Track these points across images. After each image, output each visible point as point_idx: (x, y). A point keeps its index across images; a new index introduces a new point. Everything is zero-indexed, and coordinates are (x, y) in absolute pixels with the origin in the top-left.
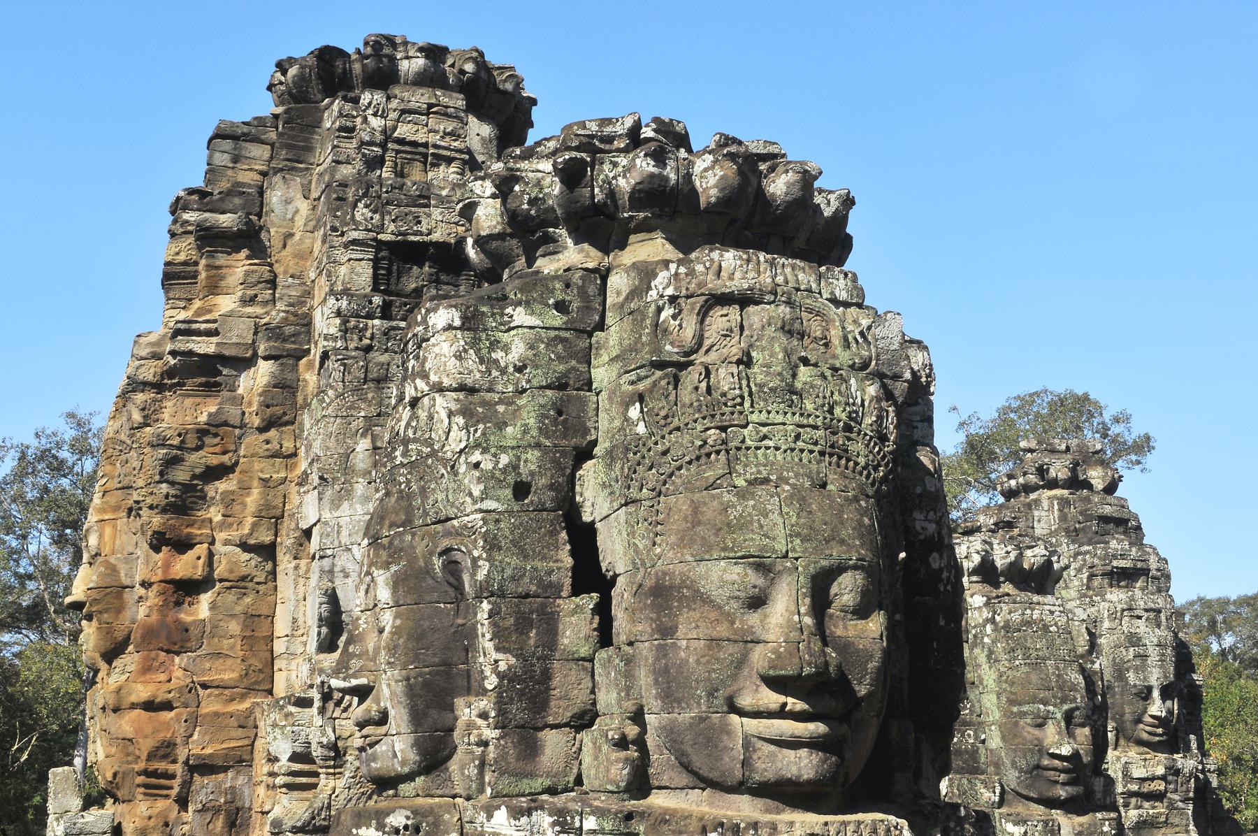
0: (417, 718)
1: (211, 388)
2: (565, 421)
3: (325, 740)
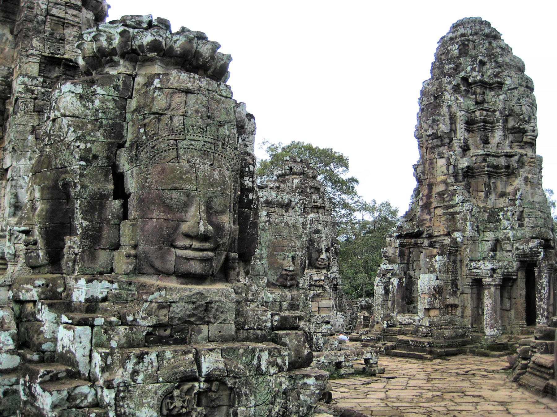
2: (114, 132)
3: (11, 252)
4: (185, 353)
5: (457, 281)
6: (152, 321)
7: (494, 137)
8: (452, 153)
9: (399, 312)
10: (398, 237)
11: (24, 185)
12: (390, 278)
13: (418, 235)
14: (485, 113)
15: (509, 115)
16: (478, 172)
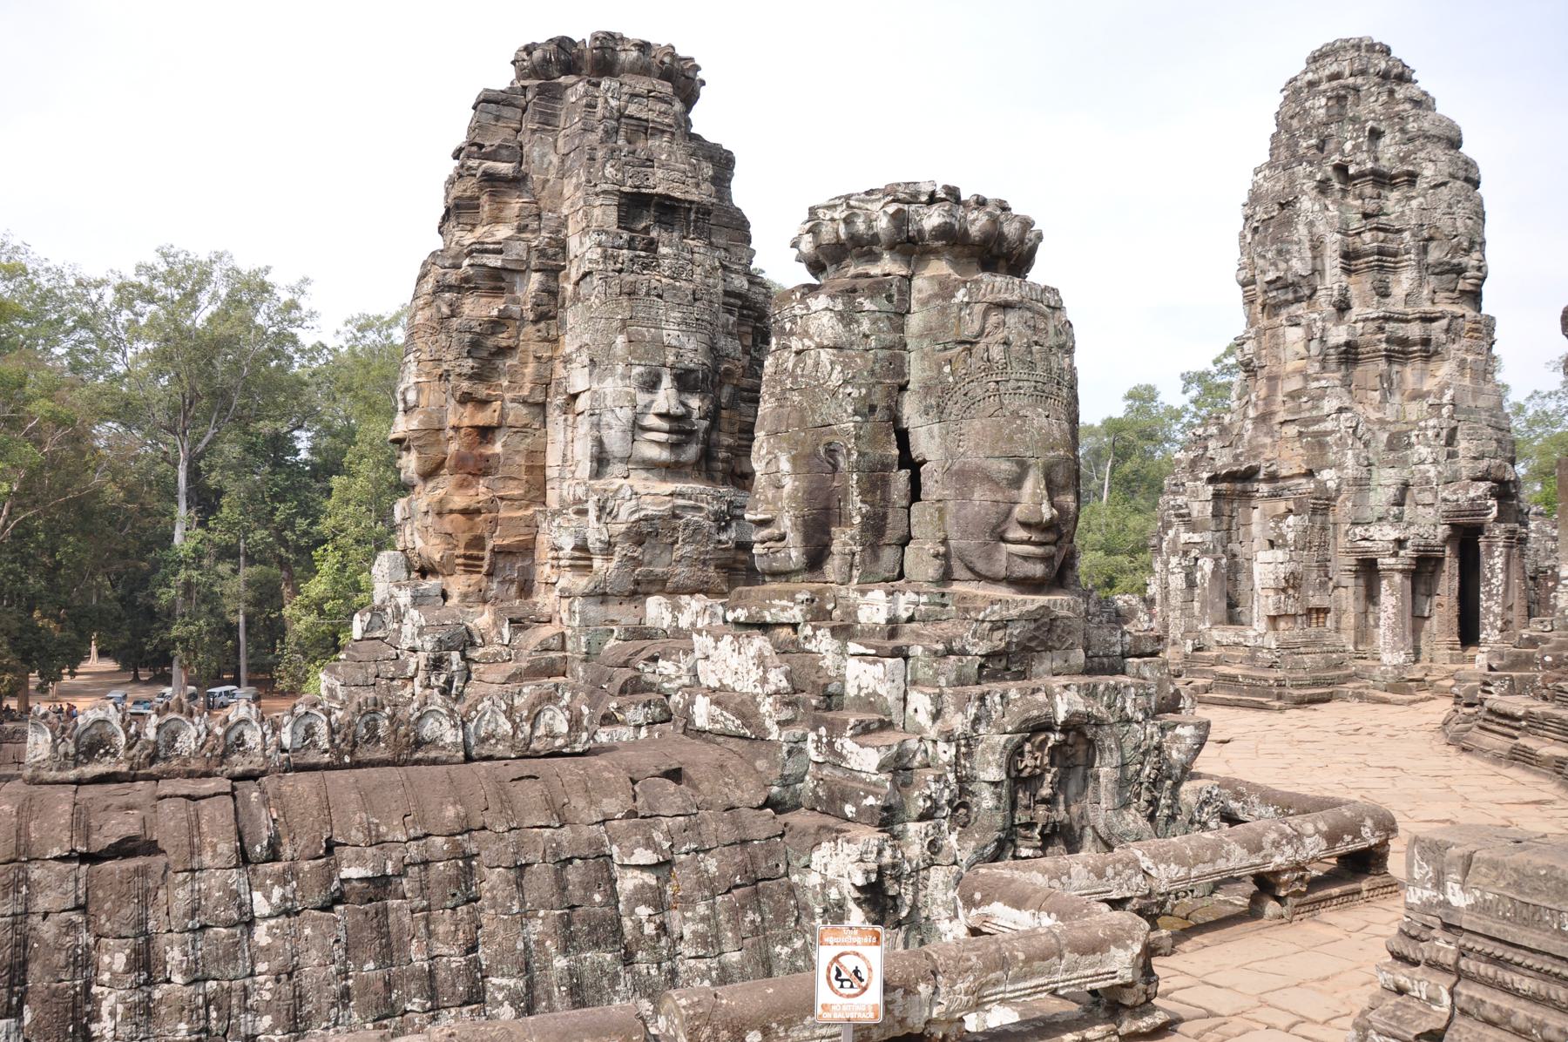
0: (807, 538)
1: (497, 291)
4: (1034, 692)
6: (984, 647)
7: (1399, 282)
8: (1315, 316)
9: (1215, 623)
10: (1211, 480)
11: (613, 422)
12: (1196, 559)
13: (1250, 475)
14: (1381, 235)
15: (1431, 239)
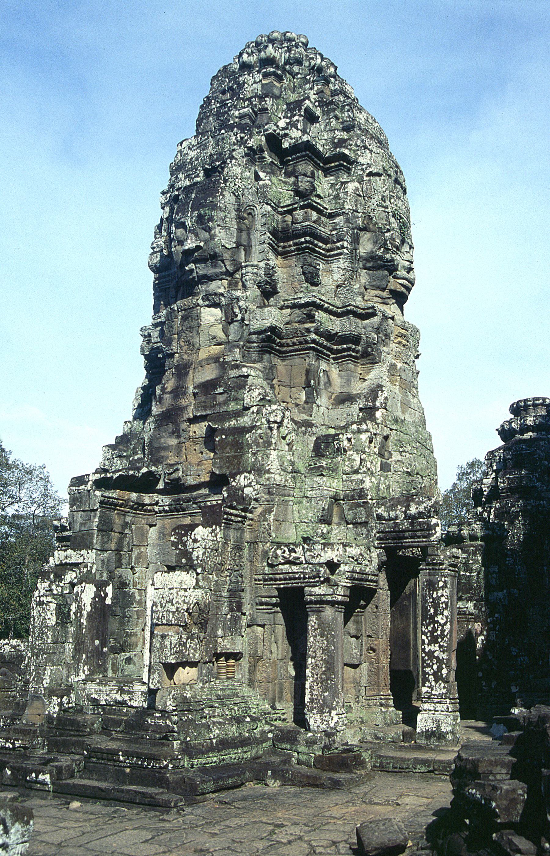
5: (243, 594)
16: (294, 344)
